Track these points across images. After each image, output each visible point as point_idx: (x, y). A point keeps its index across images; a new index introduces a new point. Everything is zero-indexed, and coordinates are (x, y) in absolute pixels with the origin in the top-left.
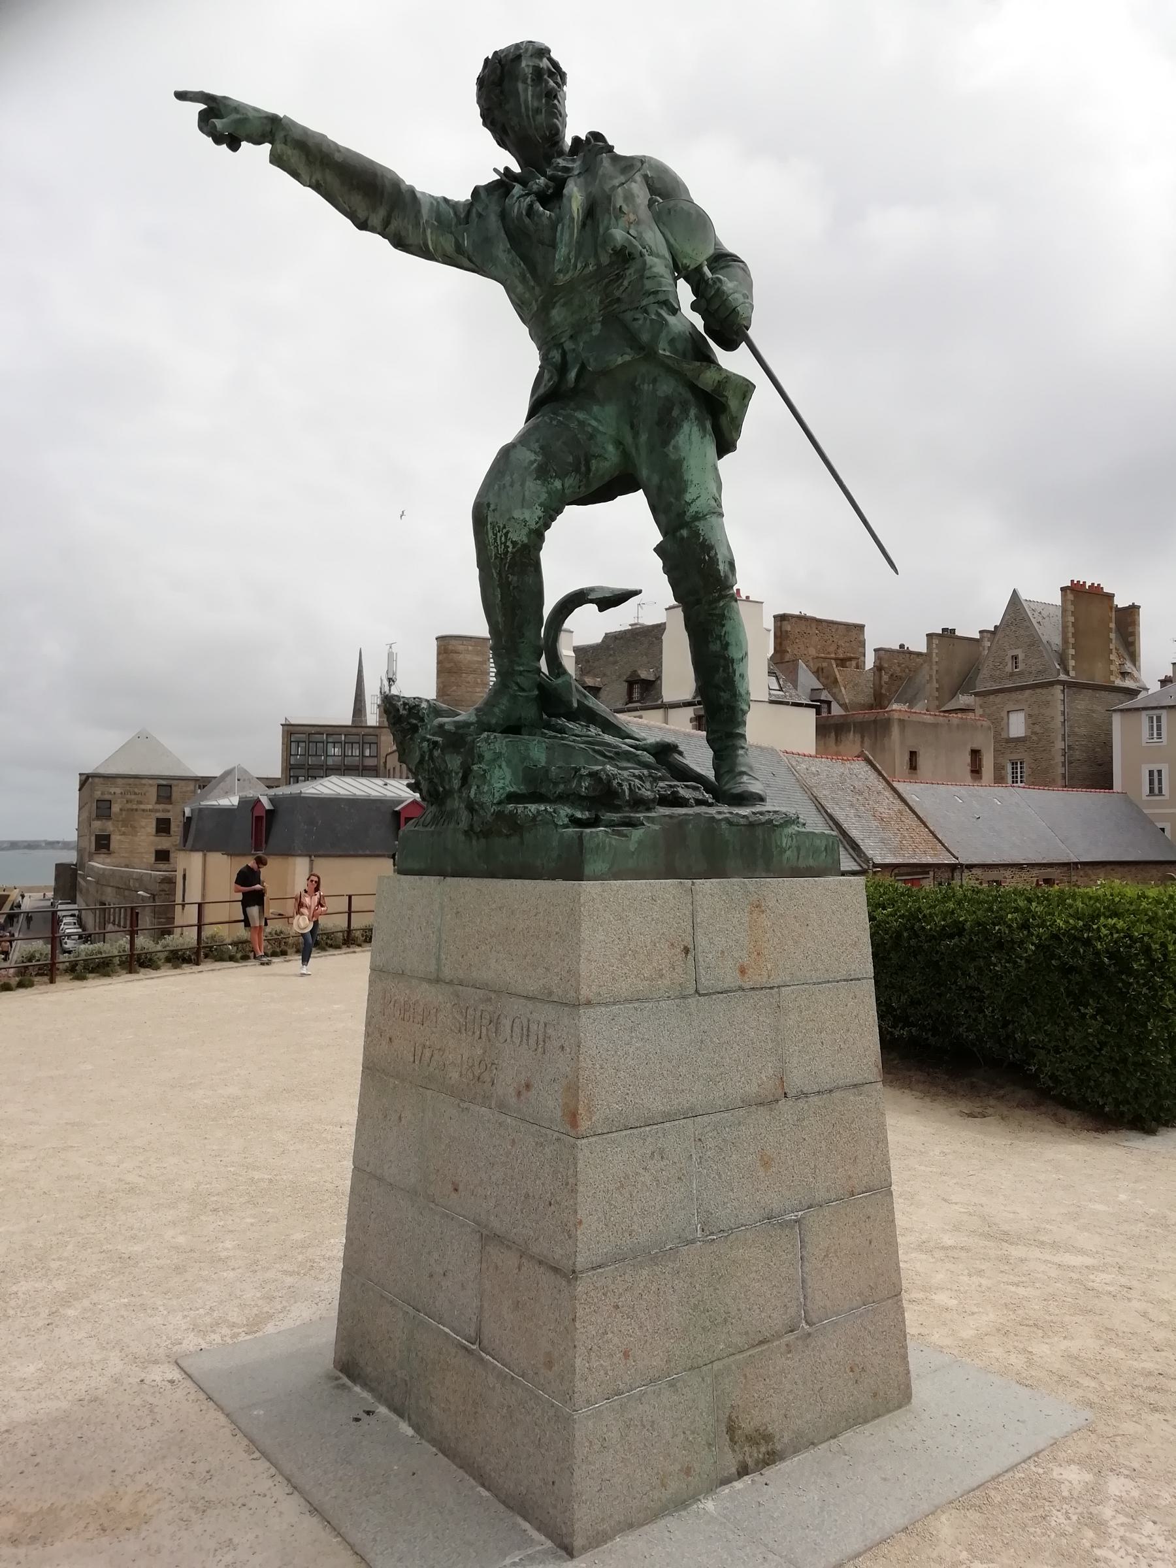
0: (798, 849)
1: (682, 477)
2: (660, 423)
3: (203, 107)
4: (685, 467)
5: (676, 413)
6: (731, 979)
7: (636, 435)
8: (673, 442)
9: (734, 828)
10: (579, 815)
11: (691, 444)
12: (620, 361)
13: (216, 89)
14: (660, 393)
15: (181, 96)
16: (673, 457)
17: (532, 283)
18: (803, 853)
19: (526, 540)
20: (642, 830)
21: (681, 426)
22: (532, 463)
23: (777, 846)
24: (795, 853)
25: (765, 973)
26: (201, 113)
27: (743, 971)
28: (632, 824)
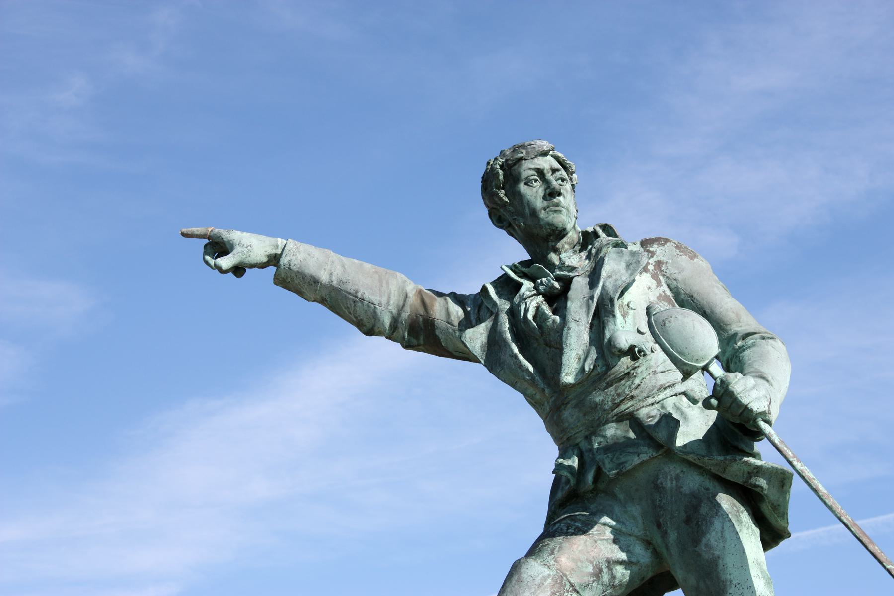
1: (718, 578)
2: (688, 521)
3: (207, 241)
4: (721, 567)
5: (704, 509)
7: (664, 535)
8: (704, 541)
11: (724, 541)
12: (636, 461)
14: (686, 489)
16: (706, 556)
17: (542, 386)
21: (712, 523)
22: (545, 579)
26: (205, 246)
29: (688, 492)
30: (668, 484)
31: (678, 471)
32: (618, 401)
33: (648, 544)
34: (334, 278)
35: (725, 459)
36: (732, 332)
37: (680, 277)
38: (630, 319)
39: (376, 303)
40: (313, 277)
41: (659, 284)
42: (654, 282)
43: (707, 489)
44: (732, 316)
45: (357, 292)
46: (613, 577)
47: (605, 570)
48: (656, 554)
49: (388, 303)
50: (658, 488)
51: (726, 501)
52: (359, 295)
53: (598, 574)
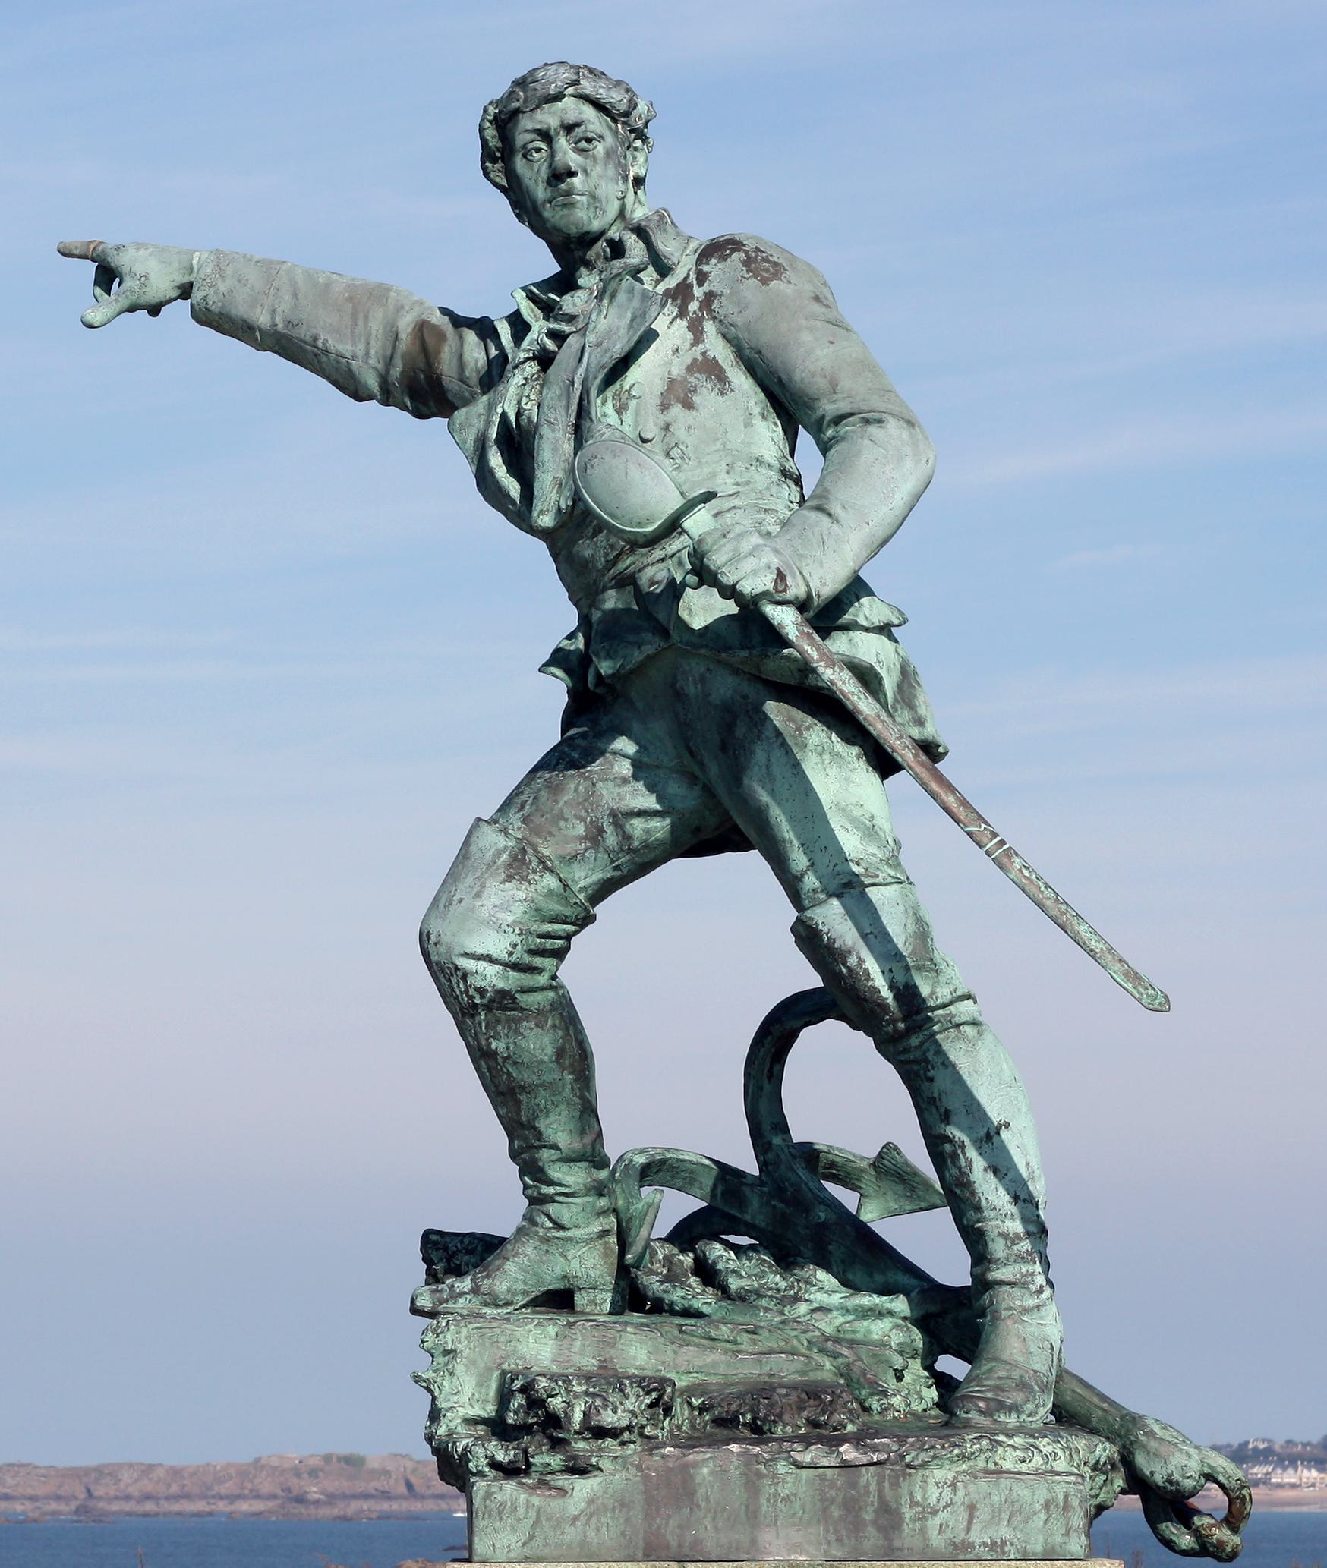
0: (972, 1508)
2: (724, 747)
5: (740, 731)
7: (702, 765)
9: (805, 1473)
10: (500, 1457)
13: (108, 237)
15: (66, 254)
18: (982, 1515)
19: (500, 985)
20: (599, 1480)
21: (752, 753)
22: (498, 854)
23: (914, 1504)
24: (963, 1515)
29: (718, 702)
30: (691, 690)
31: (703, 669)
32: (611, 557)
33: (692, 779)
34: (278, 320)
35: (750, 654)
36: (820, 412)
37: (739, 320)
38: (628, 417)
39: (348, 355)
40: (244, 321)
41: (698, 336)
42: (690, 336)
43: (745, 697)
44: (822, 383)
45: (315, 339)
46: (627, 838)
47: (609, 829)
48: (708, 791)
49: (367, 354)
50: (679, 695)
51: (776, 711)
52: (320, 344)
53: (595, 836)
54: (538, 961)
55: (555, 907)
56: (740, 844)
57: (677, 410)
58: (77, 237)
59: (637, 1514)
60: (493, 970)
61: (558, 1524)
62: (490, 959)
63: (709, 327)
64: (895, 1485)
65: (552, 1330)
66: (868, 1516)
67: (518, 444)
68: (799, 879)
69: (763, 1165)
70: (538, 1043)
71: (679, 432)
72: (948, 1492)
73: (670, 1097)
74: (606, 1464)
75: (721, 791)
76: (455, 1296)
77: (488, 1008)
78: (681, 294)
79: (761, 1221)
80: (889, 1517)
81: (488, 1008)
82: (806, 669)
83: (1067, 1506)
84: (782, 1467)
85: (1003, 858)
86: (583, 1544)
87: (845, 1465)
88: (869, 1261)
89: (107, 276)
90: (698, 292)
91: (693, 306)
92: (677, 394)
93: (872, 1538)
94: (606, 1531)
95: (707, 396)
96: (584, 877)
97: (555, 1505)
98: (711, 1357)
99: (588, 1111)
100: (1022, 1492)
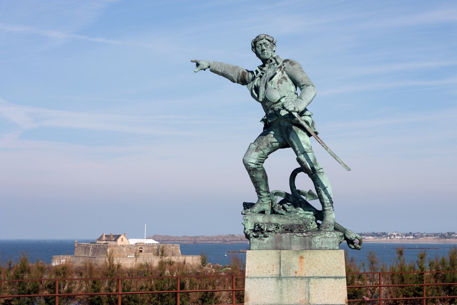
0: (322, 242)
2: (286, 133)
5: (289, 130)
6: (293, 274)
13: (198, 59)
14: (285, 126)
18: (324, 243)
24: (321, 243)
25: (304, 274)
27: (296, 272)
28: (265, 237)
30: (282, 124)
33: (282, 137)
38: (273, 85)
44: (301, 80)
46: (273, 146)
48: (284, 139)
50: (280, 125)
51: (294, 127)
53: (268, 146)
54: (260, 163)
55: (262, 156)
56: (289, 147)
57: (280, 84)
58: (193, 59)
59: (274, 243)
60: (253, 165)
61: (263, 244)
62: (253, 163)
63: (284, 72)
64: (311, 239)
65: (262, 217)
66: (307, 243)
67: (257, 89)
68: (297, 152)
69: (292, 193)
70: (260, 175)
71: (280, 87)
72: (319, 240)
73: (279, 183)
74: (269, 236)
75: (286, 139)
76: (248, 212)
77: (253, 170)
78: (280, 67)
79: (292, 201)
80: (310, 244)
81: (253, 170)
82: (298, 121)
83: (336, 242)
84: (295, 236)
85: (327, 149)
86: (266, 247)
87: (304, 236)
88: (307, 207)
89: (198, 65)
90: (283, 67)
91: (282, 69)
92: (280, 82)
93: (308, 247)
94: (270, 246)
95: (284, 82)
96: (266, 151)
97: (262, 242)
98: (285, 221)
99: (267, 185)
100: (329, 240)
